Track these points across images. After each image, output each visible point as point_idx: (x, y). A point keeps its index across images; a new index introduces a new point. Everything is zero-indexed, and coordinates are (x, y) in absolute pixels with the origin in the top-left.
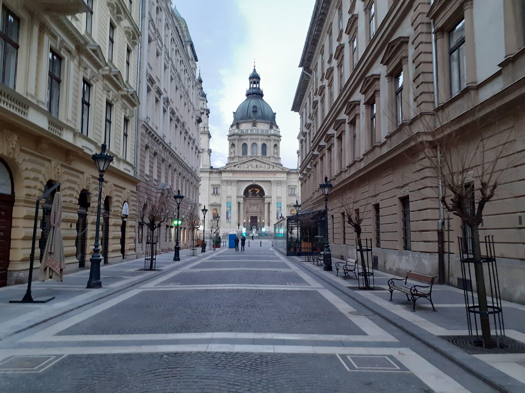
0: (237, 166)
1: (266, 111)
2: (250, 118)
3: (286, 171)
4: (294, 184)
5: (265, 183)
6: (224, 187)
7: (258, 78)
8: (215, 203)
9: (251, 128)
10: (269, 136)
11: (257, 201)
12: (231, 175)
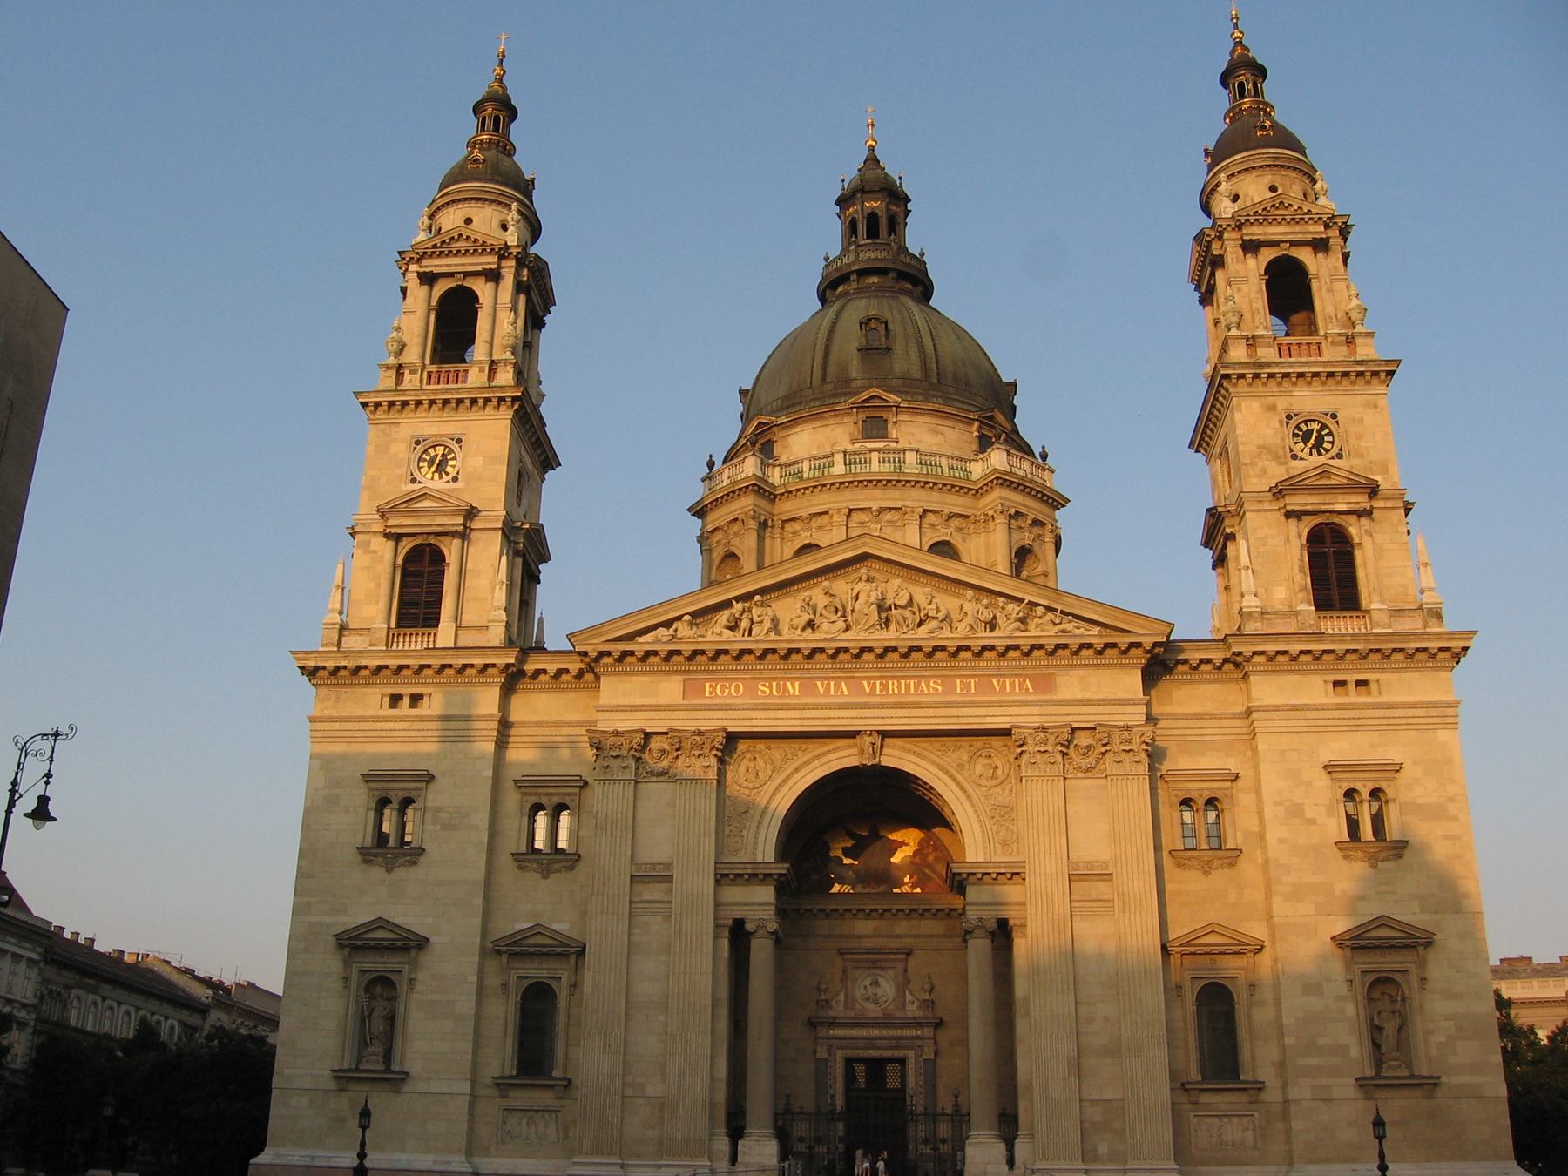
0: (724, 617)
1: (948, 345)
2: (843, 387)
3: (1139, 645)
4: (1211, 761)
5: (964, 755)
6: (615, 790)
7: (897, 197)
8: (538, 930)
9: (850, 447)
10: (978, 493)
11: (902, 927)
12: (669, 689)
